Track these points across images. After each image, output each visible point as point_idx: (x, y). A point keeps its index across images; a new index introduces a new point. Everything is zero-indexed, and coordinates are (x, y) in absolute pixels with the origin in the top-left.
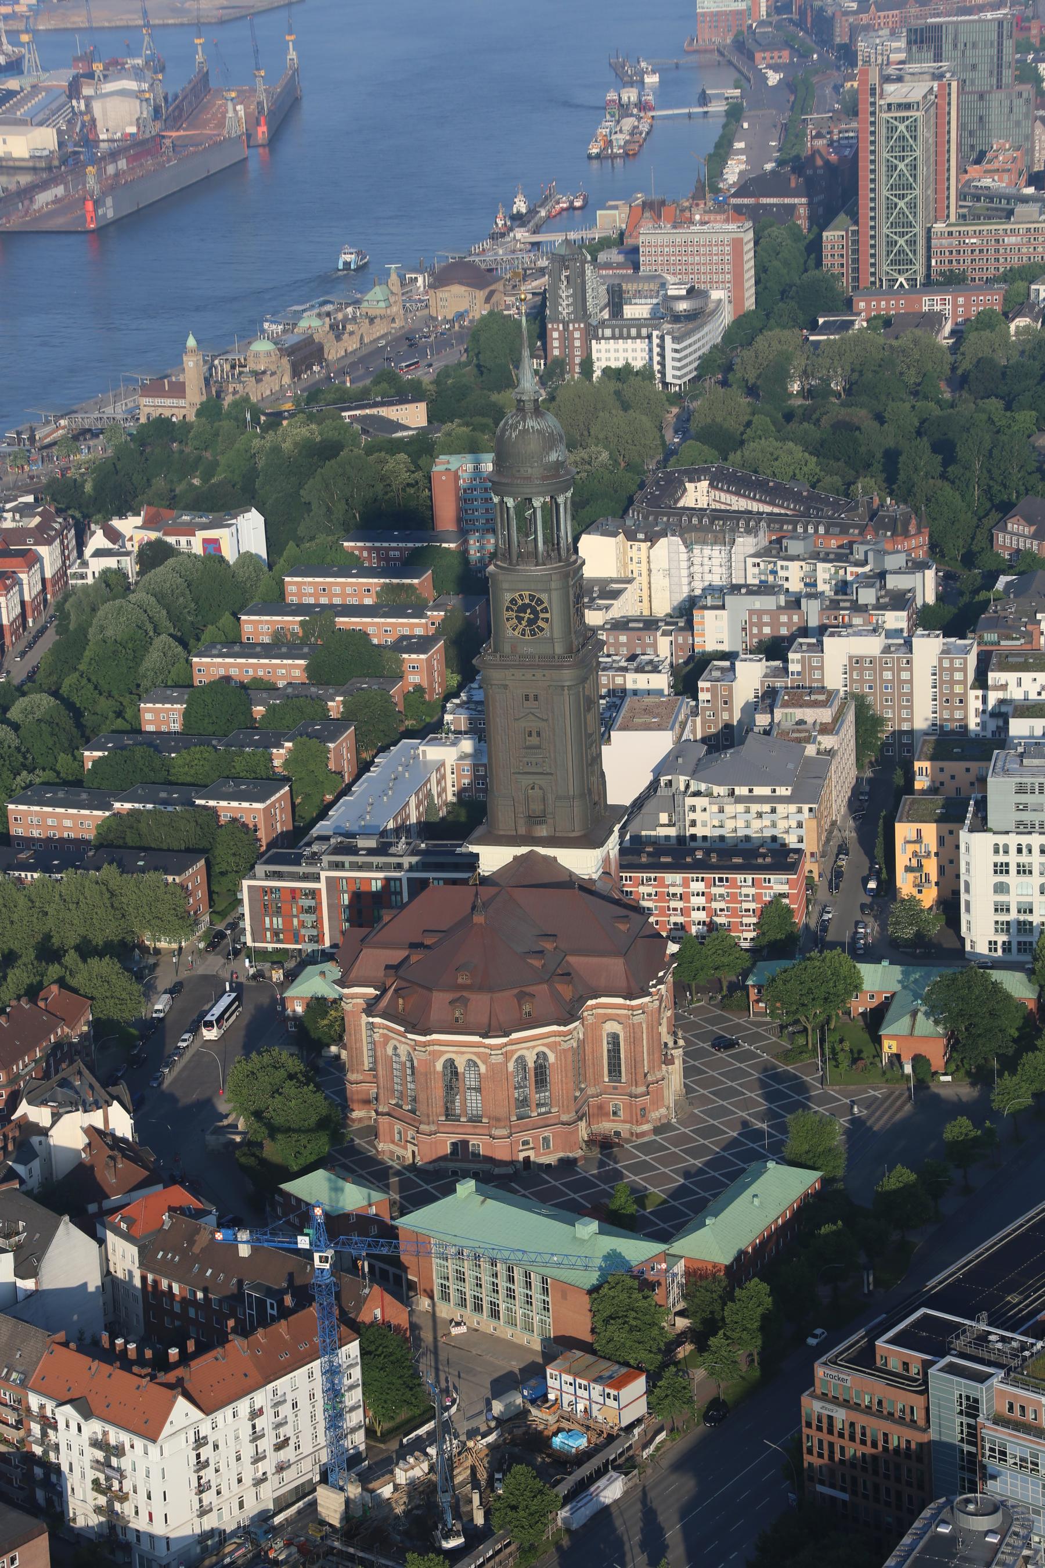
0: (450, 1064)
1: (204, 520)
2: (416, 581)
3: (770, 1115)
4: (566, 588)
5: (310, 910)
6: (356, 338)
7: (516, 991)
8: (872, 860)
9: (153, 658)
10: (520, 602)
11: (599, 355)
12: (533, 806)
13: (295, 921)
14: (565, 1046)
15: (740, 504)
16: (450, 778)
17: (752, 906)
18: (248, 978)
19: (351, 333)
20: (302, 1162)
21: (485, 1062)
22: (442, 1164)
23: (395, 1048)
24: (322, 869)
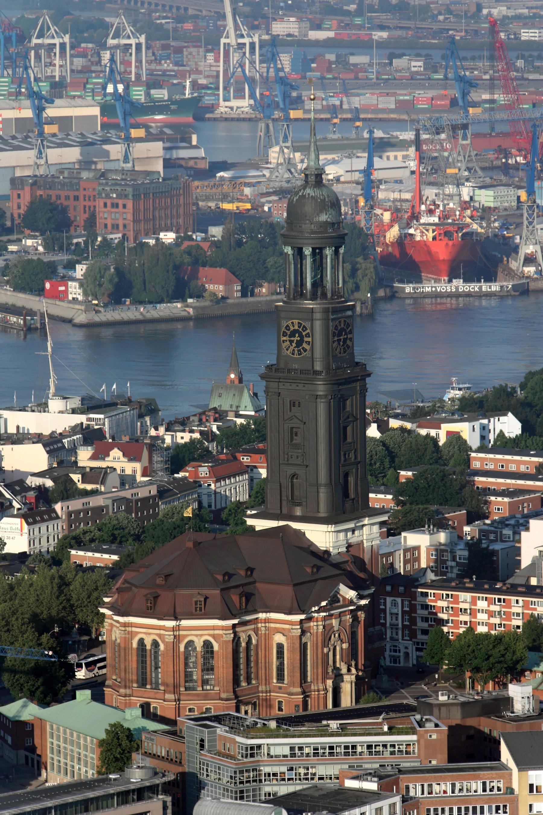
0: (141, 642)
12: (296, 493)
14: (225, 638)
21: (163, 642)
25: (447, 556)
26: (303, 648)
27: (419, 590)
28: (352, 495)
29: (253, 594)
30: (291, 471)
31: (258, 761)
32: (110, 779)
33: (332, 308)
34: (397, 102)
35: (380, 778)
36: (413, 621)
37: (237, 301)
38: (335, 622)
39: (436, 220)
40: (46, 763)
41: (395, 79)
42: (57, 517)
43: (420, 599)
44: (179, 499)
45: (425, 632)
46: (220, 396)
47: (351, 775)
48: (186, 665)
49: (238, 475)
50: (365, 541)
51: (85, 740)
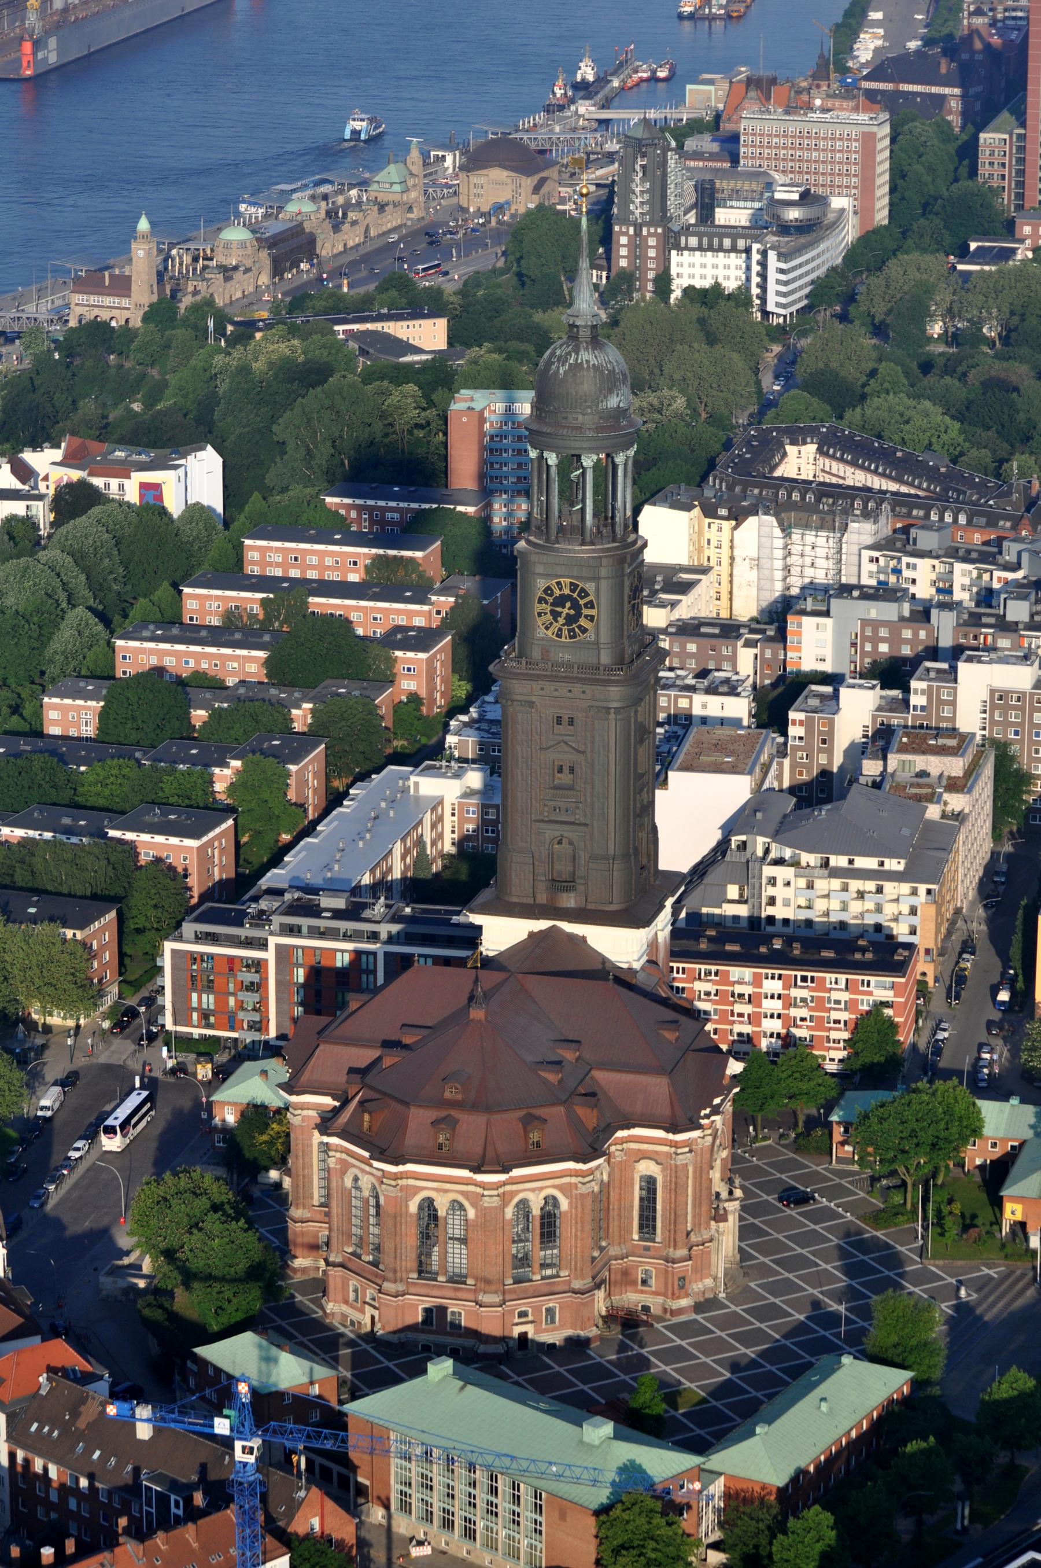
0: (428, 1205)
1: (143, 458)
2: (419, 554)
3: (849, 1294)
4: (620, 577)
5: (251, 987)
6: (360, 230)
7: (522, 1113)
8: (1006, 964)
9: (64, 638)
10: (557, 593)
11: (680, 270)
12: (558, 867)
13: (232, 1001)
14: (584, 1190)
15: (856, 477)
16: (449, 821)
17: (844, 1016)
18: (165, 1072)
19: (354, 223)
20: (225, 1320)
21: (474, 1205)
22: (410, 1335)
23: (356, 1179)
24: (272, 933)
40: (388, 1499)
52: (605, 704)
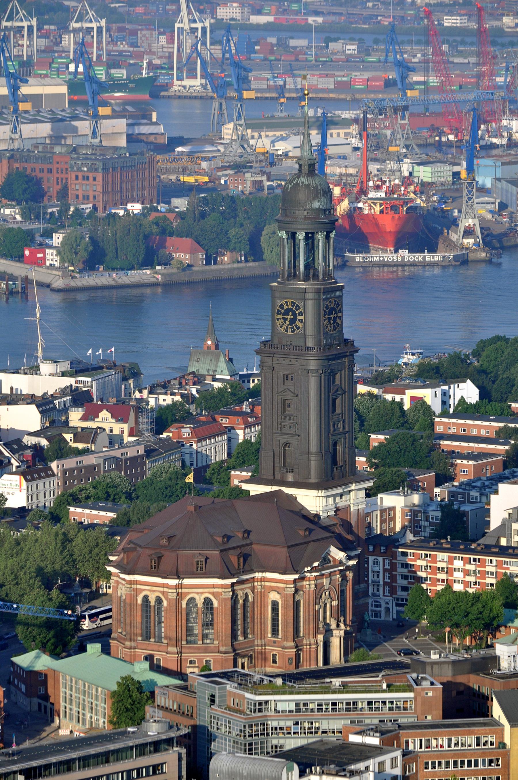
0: (146, 598)
10: (286, 307)
12: (288, 460)
14: (224, 596)
21: (166, 598)
25: (421, 516)
26: (296, 605)
27: (400, 550)
28: (340, 462)
29: (250, 555)
30: (284, 439)
31: (266, 716)
32: (129, 732)
33: (324, 288)
34: (336, 83)
35: (382, 733)
36: (393, 578)
37: (201, 268)
38: (325, 581)
39: (383, 195)
40: (59, 711)
41: (332, 61)
42: (53, 475)
43: (400, 558)
44: (164, 458)
45: (405, 589)
46: (198, 361)
47: (355, 731)
48: (188, 620)
49: (218, 435)
50: (352, 505)
51: (97, 691)
52: (306, 368)
